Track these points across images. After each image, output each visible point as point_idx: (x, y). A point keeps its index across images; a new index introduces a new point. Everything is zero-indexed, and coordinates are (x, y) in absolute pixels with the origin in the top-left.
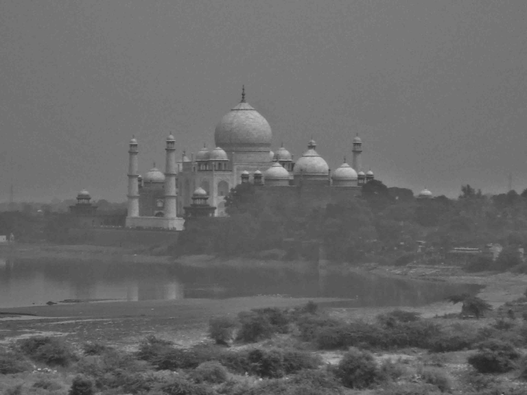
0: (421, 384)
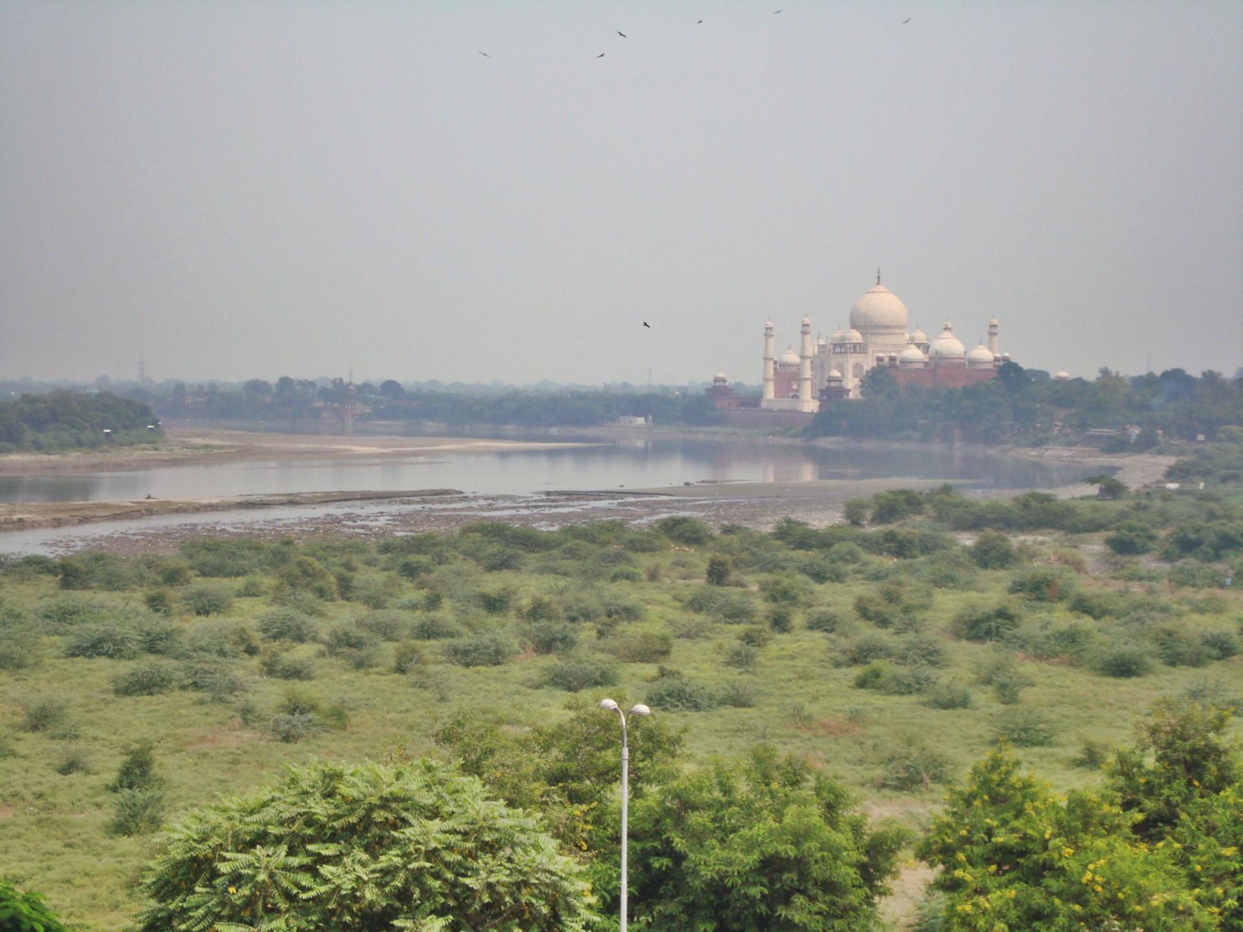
0: (1057, 565)
